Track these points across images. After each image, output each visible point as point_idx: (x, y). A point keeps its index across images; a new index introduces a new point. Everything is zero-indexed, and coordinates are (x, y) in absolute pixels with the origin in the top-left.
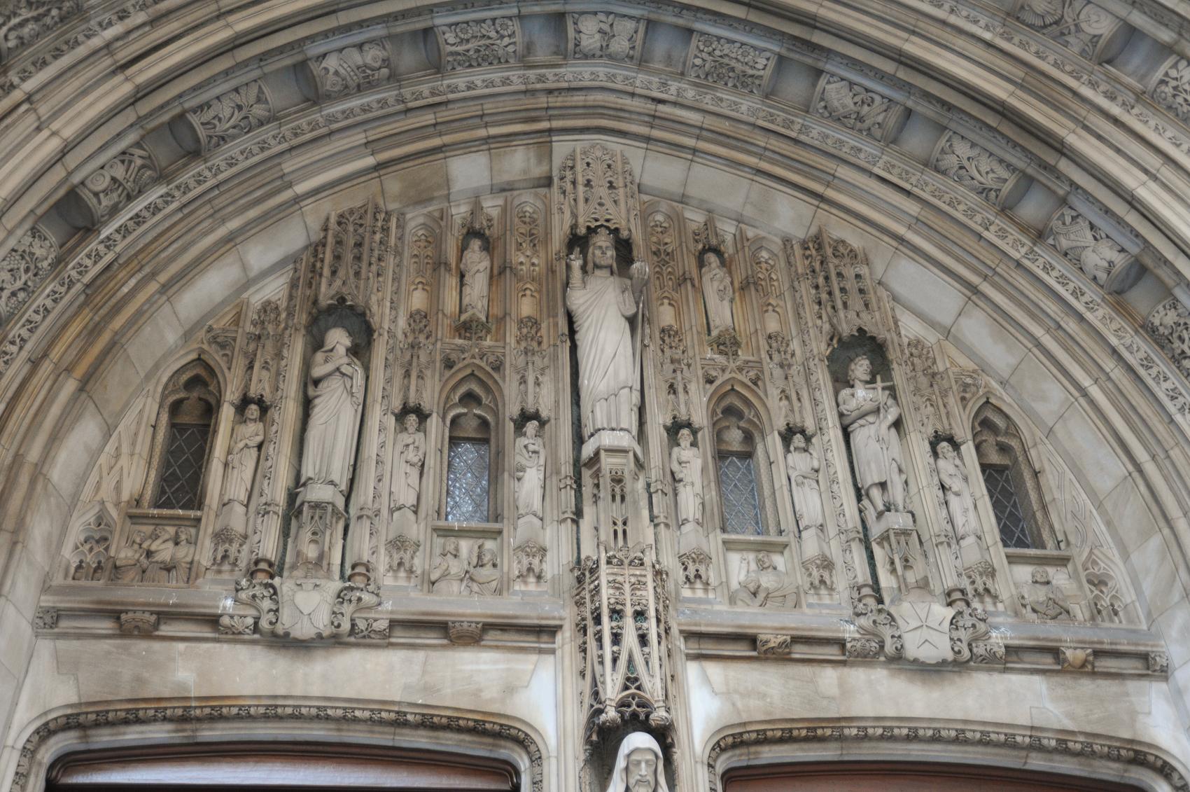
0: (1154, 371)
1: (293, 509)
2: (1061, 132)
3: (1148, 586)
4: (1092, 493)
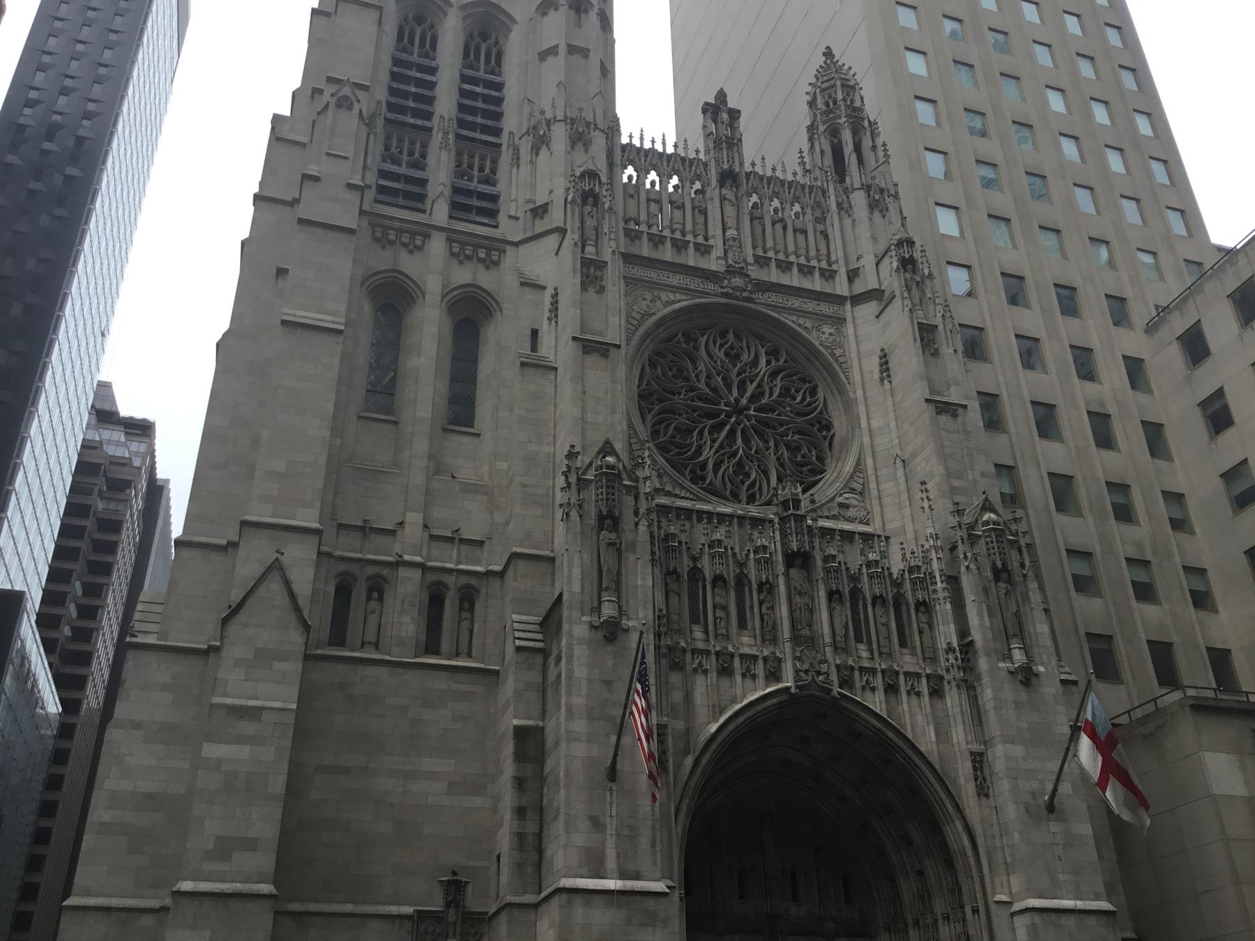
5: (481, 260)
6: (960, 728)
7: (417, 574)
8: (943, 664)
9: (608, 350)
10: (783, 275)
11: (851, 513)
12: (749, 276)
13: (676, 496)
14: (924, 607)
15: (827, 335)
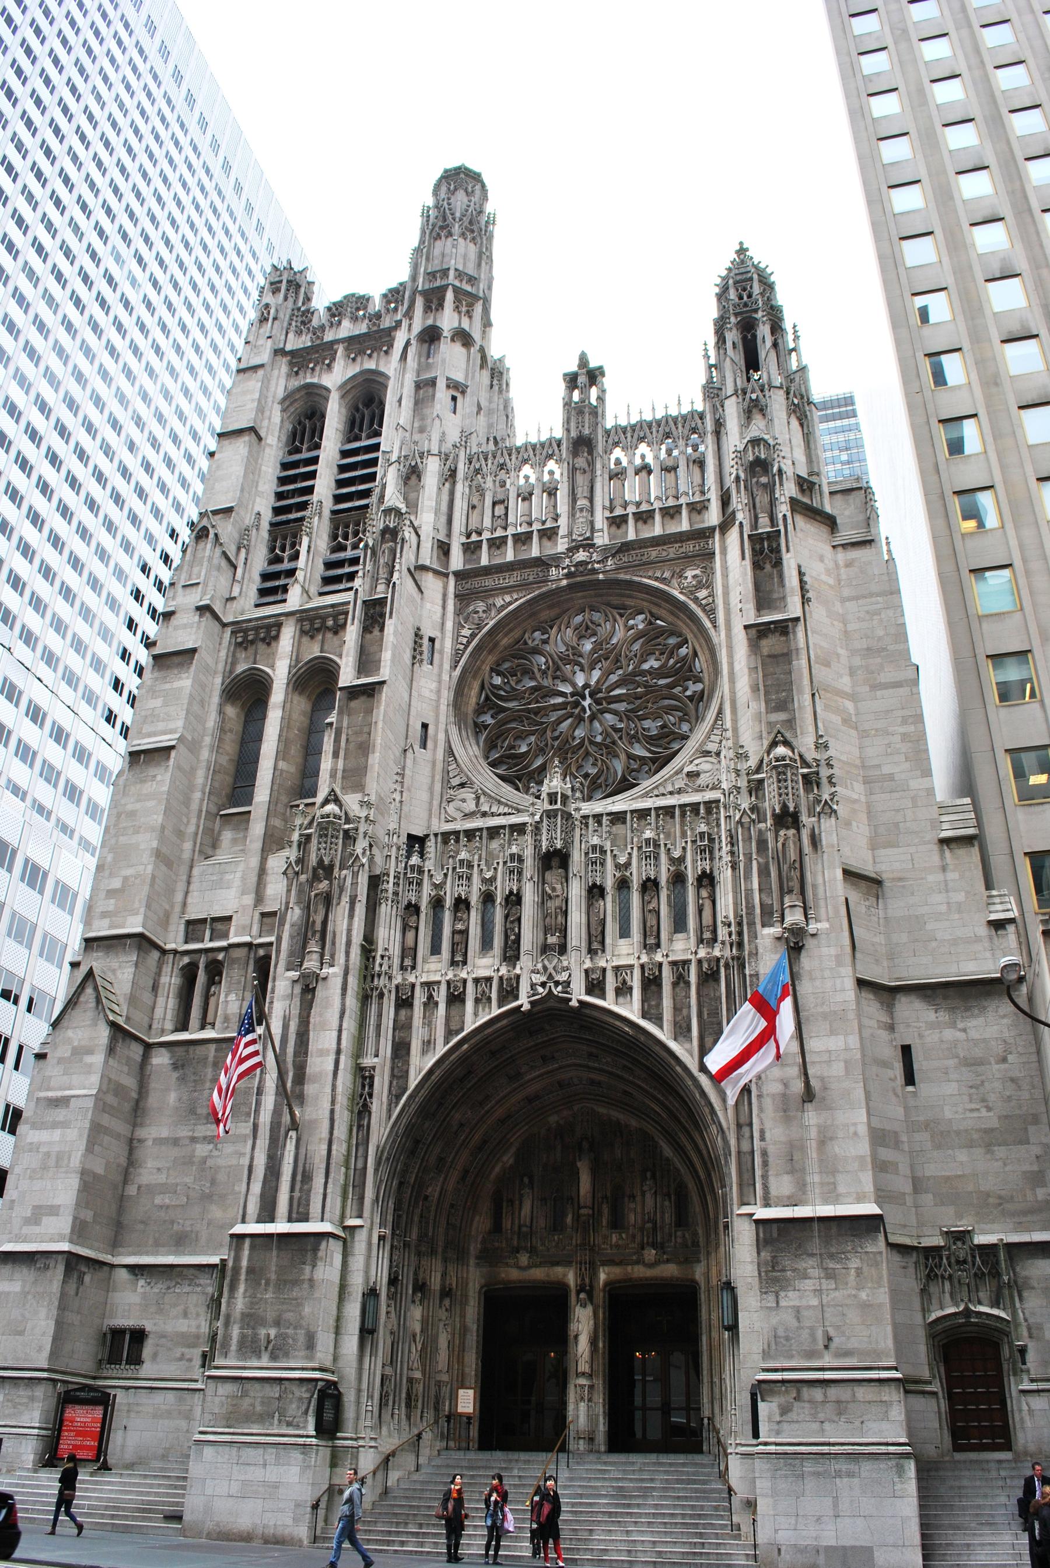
1: (519, 1233)
5: (329, 629)
7: (244, 951)
9: (373, 690)
10: (645, 527)
11: (702, 780)
12: (593, 546)
13: (493, 815)
14: (707, 880)
15: (689, 580)
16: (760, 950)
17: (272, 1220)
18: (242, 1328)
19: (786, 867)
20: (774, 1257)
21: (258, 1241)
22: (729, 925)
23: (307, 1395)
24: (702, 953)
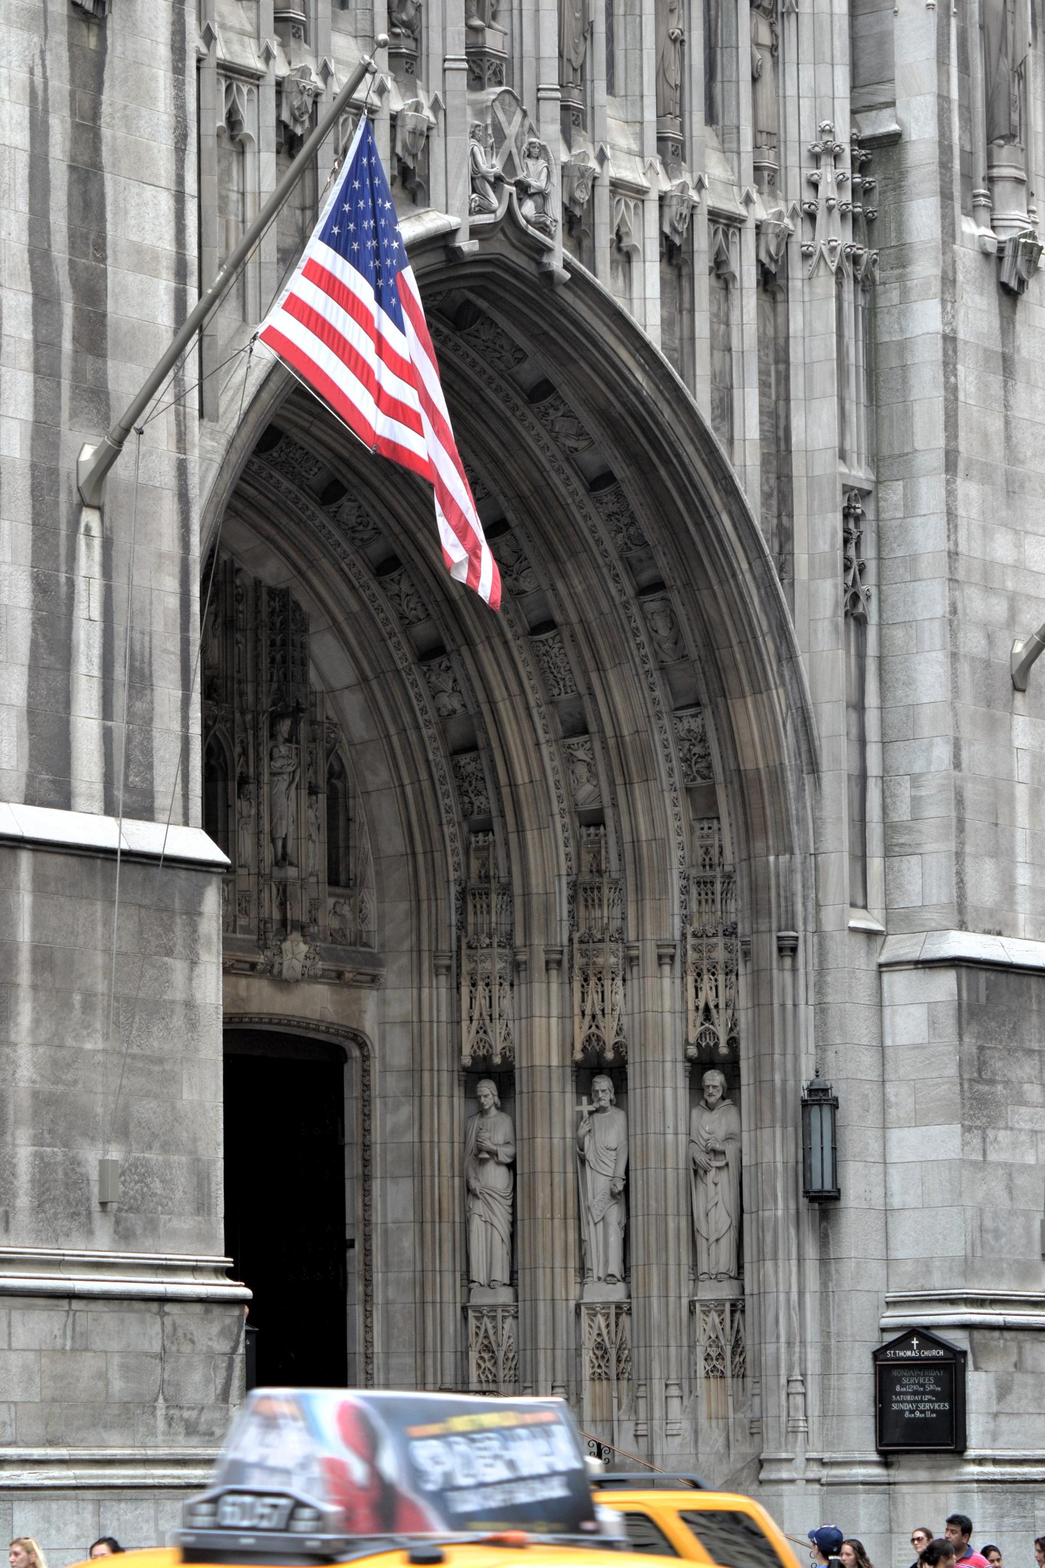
0: (444, 788)
2: (477, 640)
3: (388, 930)
4: (376, 848)
6: (827, 411)
8: (796, 192)
16: (960, 277)
17: (64, 801)
18: (38, 1141)
19: (1005, 65)
20: (981, 1049)
21: (55, 862)
22: (837, 157)
23: (224, 1346)
24: (761, 211)
